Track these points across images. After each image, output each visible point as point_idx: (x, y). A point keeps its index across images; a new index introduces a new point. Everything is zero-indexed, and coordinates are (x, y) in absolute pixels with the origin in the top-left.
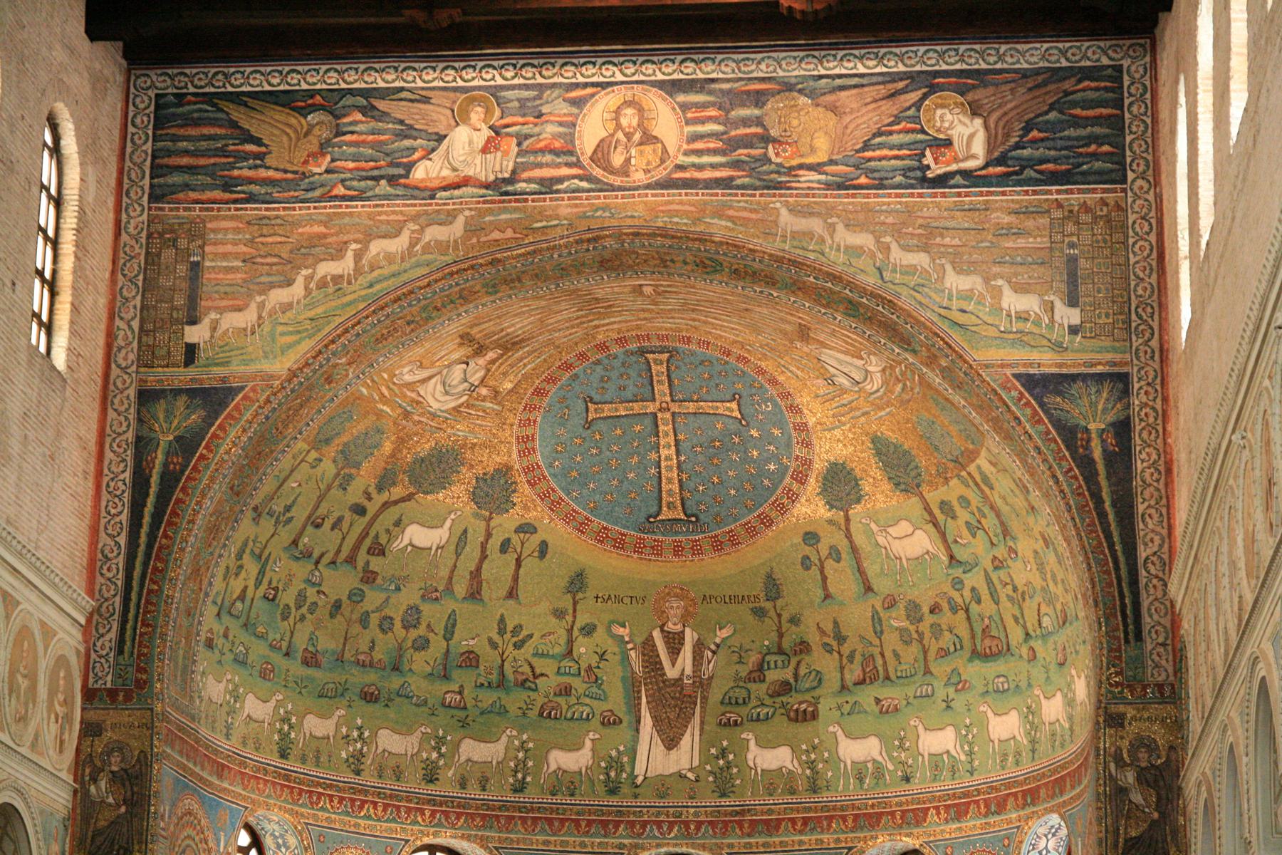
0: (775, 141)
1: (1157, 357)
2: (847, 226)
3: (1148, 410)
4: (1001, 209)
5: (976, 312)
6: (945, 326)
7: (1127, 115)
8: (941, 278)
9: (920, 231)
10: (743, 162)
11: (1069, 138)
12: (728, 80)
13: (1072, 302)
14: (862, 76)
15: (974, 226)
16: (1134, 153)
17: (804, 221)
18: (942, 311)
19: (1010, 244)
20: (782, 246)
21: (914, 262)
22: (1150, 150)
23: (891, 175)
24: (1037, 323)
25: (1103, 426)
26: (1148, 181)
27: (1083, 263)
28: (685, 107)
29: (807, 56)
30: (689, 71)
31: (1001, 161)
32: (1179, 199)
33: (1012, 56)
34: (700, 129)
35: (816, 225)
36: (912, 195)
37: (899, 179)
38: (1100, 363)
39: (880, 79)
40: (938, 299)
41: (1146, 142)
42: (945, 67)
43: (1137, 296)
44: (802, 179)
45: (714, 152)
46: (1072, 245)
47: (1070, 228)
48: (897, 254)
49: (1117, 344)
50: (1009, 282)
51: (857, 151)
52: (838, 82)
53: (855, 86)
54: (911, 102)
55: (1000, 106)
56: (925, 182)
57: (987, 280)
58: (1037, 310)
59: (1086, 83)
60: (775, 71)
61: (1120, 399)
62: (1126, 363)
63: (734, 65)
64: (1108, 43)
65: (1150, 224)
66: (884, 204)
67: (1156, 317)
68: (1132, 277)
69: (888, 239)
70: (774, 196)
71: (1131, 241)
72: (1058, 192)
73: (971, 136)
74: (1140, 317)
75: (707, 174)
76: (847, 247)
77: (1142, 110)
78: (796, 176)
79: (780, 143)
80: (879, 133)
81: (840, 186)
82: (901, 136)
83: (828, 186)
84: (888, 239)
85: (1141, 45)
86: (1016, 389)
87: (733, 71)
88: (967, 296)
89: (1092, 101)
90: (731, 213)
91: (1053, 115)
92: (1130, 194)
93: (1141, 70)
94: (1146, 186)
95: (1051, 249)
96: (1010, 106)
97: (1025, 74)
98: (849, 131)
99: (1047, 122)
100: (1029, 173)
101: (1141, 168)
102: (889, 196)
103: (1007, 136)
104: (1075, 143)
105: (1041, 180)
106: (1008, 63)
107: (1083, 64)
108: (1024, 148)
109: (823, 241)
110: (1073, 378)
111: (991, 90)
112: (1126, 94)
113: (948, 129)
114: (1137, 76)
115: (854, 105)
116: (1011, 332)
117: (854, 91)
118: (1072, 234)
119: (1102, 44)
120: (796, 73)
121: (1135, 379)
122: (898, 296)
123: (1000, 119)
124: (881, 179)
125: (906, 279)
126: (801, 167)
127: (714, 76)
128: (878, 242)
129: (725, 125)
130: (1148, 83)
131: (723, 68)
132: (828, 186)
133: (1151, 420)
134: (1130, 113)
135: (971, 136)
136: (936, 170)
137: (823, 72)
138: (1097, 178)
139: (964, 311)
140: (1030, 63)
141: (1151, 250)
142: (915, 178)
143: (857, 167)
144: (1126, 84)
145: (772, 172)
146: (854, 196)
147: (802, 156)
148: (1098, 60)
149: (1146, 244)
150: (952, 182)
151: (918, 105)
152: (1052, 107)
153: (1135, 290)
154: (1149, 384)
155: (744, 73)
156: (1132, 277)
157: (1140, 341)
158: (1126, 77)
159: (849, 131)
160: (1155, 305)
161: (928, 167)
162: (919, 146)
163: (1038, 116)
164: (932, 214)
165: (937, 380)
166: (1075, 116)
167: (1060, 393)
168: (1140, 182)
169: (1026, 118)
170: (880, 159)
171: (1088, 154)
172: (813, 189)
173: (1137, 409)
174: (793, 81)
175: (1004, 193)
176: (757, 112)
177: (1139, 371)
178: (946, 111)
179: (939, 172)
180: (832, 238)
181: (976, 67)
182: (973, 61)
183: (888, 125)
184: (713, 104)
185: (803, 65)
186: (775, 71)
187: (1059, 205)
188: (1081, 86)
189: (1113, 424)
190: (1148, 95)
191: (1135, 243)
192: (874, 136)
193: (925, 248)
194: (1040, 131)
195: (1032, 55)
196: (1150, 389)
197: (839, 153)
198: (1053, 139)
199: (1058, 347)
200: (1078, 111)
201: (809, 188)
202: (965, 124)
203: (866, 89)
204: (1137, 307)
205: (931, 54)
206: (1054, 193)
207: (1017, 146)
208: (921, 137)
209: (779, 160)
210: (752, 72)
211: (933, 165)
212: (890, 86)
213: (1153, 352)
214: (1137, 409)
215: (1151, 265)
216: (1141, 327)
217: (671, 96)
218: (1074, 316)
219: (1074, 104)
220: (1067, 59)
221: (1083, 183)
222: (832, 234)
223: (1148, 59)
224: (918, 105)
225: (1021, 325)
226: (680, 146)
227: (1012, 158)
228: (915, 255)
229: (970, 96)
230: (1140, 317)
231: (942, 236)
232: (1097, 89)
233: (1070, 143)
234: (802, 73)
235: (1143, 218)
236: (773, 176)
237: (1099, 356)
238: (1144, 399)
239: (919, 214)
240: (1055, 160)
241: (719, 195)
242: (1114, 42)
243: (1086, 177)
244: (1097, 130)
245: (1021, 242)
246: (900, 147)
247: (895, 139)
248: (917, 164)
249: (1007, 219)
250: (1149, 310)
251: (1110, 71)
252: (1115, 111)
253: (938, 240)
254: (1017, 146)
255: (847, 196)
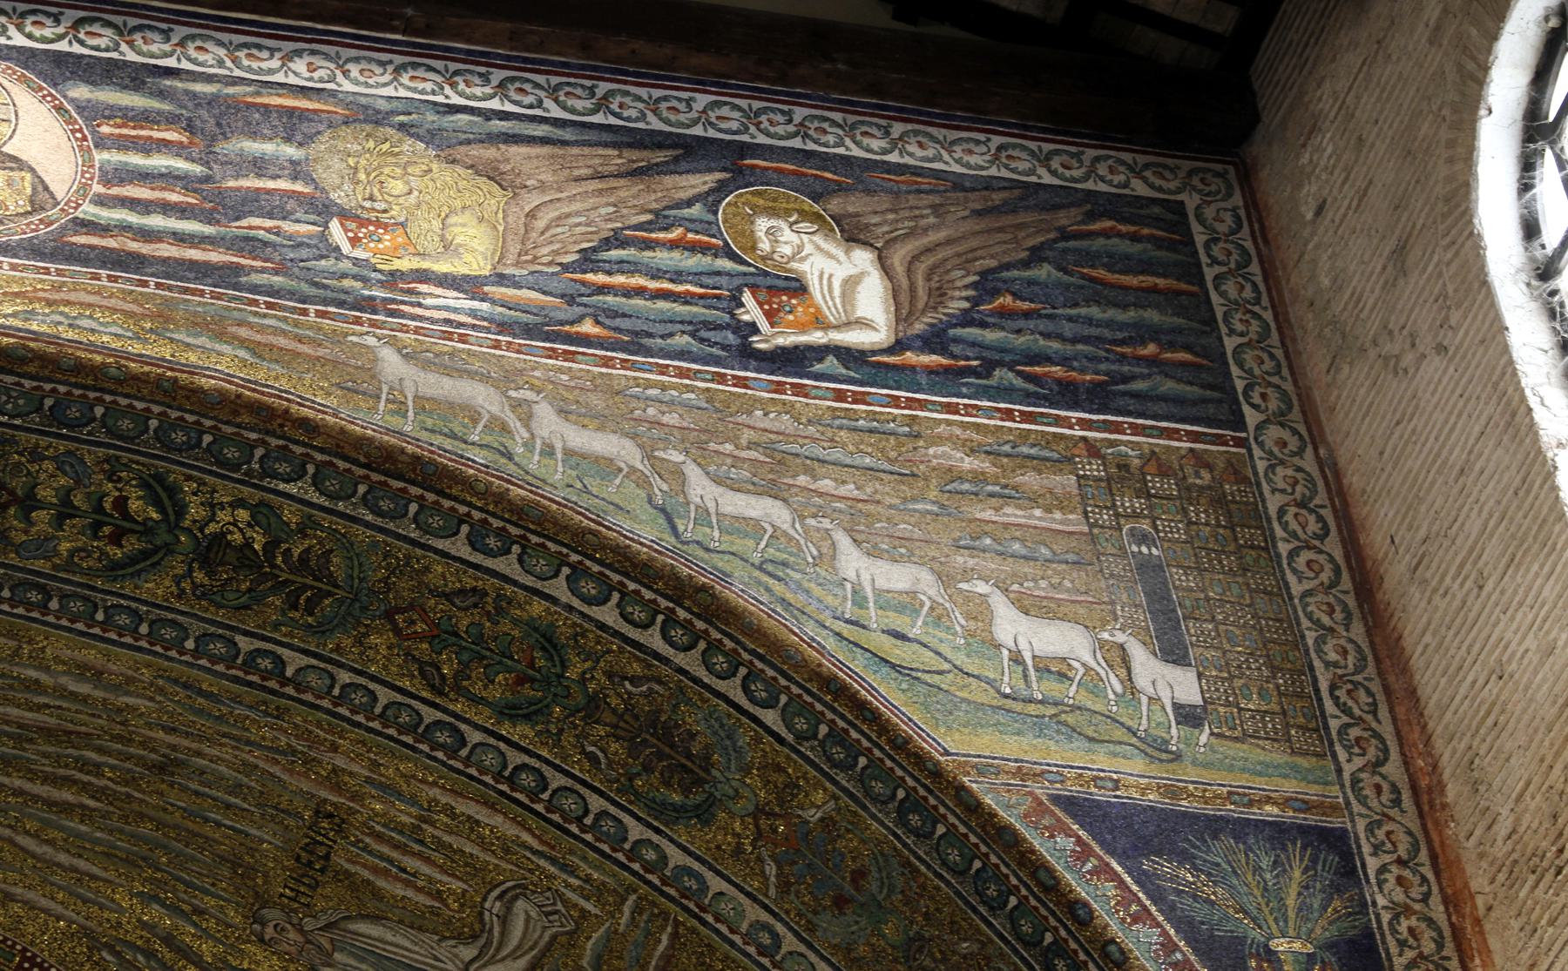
0: (344, 215)
1: (1406, 796)
2: (563, 413)
3: (1413, 922)
4: (951, 439)
5: (925, 639)
6: (858, 663)
7: (1215, 298)
8: (828, 557)
9: (753, 454)
10: (266, 244)
11: (1090, 321)
12: (210, 79)
13: (1174, 654)
14: (556, 123)
15: (887, 466)
16: (1250, 372)
17: (447, 383)
18: (839, 626)
19: (988, 515)
20: (395, 422)
21: (753, 514)
22: (1285, 372)
23: (659, 329)
24: (1093, 684)
25: (1310, 949)
26: (1295, 432)
27: (1176, 575)
28: (93, 113)
29: (415, 66)
30: (103, 42)
31: (934, 340)
32: (1510, 318)
33: (921, 145)
34: (136, 160)
35: (484, 398)
36: (721, 379)
37: (682, 340)
38: (1269, 800)
39: (606, 137)
40: (829, 600)
41: (1272, 356)
42: (762, 139)
43: (1327, 664)
44: (429, 301)
45: (182, 211)
46: (1143, 539)
47: (1128, 502)
48: (700, 488)
49: (1303, 762)
50: (1006, 591)
51: (566, 267)
52: (498, 125)
53: (544, 141)
54: (690, 193)
55: (911, 234)
56: (747, 355)
57: (945, 578)
58: (1088, 658)
59: (1108, 224)
60: (332, 79)
61: (1336, 889)
62: (1335, 808)
63: (222, 52)
64: (1142, 159)
65: (1320, 519)
66: (650, 384)
67: (1383, 712)
68: (1305, 623)
69: (676, 457)
70: (358, 321)
71: (1284, 548)
72: (1084, 424)
73: (851, 283)
74: (1347, 711)
75: (166, 250)
76: (569, 453)
77: (1248, 293)
78: (411, 292)
79: (363, 223)
80: (616, 240)
81: (529, 331)
82: (676, 254)
83: (503, 327)
84: (676, 457)
85: (1218, 175)
86: (1069, 833)
87: (221, 63)
88: (907, 603)
89: (1128, 257)
90: (243, 332)
91: (1044, 272)
92: (1257, 452)
93: (1228, 218)
94: (1293, 443)
95: (1094, 540)
96: (933, 237)
97: (958, 184)
98: (540, 224)
99: (1031, 282)
100: (1002, 375)
101: (1273, 404)
102: (663, 370)
103: (939, 295)
104: (1107, 333)
105: (1045, 398)
106: (915, 154)
107: (1089, 185)
108: (983, 325)
109: (505, 429)
110: (1214, 826)
111: (883, 201)
112: (1204, 259)
113: (791, 259)
114: (1222, 228)
115: (547, 177)
116: (1031, 701)
117: (546, 150)
118: (1135, 516)
119: (1127, 157)
120: (389, 91)
121: (1366, 849)
122: (724, 577)
123: (915, 258)
124: (636, 334)
125: (740, 545)
126: (424, 276)
127: (171, 62)
128: (649, 456)
129: (207, 164)
130: (1248, 245)
131: (193, 53)
132: (503, 327)
133: (1428, 947)
134: (1223, 294)
135: (851, 283)
136: (772, 338)
137: (457, 100)
138: (1174, 410)
139: (902, 637)
140: (968, 166)
141: (1337, 571)
142: (724, 347)
143: (570, 300)
144: (1200, 239)
145: (344, 276)
146: (569, 356)
147: (422, 255)
148: (1126, 185)
149: (1322, 558)
150: (818, 367)
151: (712, 199)
152: (1036, 256)
153: (1319, 651)
154: (1400, 862)
155: (249, 70)
156: (1305, 623)
157: (1359, 762)
158: (1196, 227)
159: (540, 224)
160: (1376, 687)
161: (753, 328)
162: (724, 281)
163: (1007, 267)
164: (776, 426)
165: (754, 913)
166: (1092, 279)
167: (1184, 857)
168: (1274, 433)
169: (980, 265)
170: (628, 292)
171: (1140, 359)
172: (461, 325)
173: (1386, 917)
174: (382, 105)
175: (951, 409)
176: (290, 151)
177: (1370, 829)
178: (783, 225)
179: (780, 341)
180: (527, 426)
181: (841, 151)
182: (831, 139)
183: (639, 227)
184: (171, 120)
185: (405, 79)
186: (332, 79)
187: (1093, 450)
188: (1097, 226)
189: (1330, 946)
190: (1255, 268)
191: (1292, 554)
192: (607, 243)
193: (774, 491)
194: (1015, 295)
195: (971, 152)
196: (1407, 873)
197: (517, 264)
198: (1049, 317)
199: (1156, 748)
200: (1100, 273)
201: (448, 322)
202: (831, 256)
203: (575, 151)
204: (1333, 688)
205: (725, 111)
206: (1074, 423)
207: (966, 319)
208: (725, 264)
209: (359, 253)
210: (271, 72)
211: (763, 324)
212: (635, 154)
213: (1395, 789)
214: (1386, 917)
215: (1345, 606)
216: (1354, 732)
217: (55, 85)
218: (1185, 686)
219: (1091, 258)
220: (1054, 173)
221: (1140, 416)
222: (527, 420)
223: (1237, 199)
224: (712, 199)
225: (1052, 688)
226: (85, 187)
227: (957, 340)
228: (753, 500)
229: (835, 204)
230: (1347, 711)
231: (808, 471)
232: (1135, 238)
233: (1094, 331)
234: (402, 93)
235: (1302, 504)
236: (347, 283)
237: (1260, 782)
238: (1399, 895)
239: (743, 418)
240: (1064, 361)
241: (206, 299)
242: (1151, 158)
243: (1143, 404)
244: (1152, 316)
245: (1012, 514)
246: (677, 276)
247: (662, 258)
248: (727, 318)
249: (968, 463)
250: (1363, 697)
251: (1157, 210)
252: (1184, 286)
253: (802, 480)
254: (966, 319)
255: (552, 354)
